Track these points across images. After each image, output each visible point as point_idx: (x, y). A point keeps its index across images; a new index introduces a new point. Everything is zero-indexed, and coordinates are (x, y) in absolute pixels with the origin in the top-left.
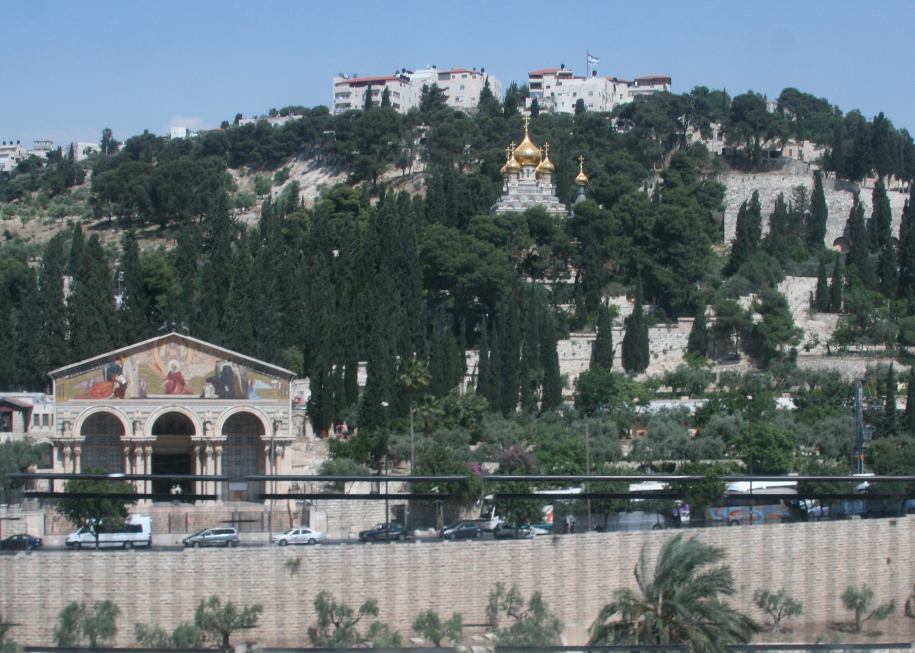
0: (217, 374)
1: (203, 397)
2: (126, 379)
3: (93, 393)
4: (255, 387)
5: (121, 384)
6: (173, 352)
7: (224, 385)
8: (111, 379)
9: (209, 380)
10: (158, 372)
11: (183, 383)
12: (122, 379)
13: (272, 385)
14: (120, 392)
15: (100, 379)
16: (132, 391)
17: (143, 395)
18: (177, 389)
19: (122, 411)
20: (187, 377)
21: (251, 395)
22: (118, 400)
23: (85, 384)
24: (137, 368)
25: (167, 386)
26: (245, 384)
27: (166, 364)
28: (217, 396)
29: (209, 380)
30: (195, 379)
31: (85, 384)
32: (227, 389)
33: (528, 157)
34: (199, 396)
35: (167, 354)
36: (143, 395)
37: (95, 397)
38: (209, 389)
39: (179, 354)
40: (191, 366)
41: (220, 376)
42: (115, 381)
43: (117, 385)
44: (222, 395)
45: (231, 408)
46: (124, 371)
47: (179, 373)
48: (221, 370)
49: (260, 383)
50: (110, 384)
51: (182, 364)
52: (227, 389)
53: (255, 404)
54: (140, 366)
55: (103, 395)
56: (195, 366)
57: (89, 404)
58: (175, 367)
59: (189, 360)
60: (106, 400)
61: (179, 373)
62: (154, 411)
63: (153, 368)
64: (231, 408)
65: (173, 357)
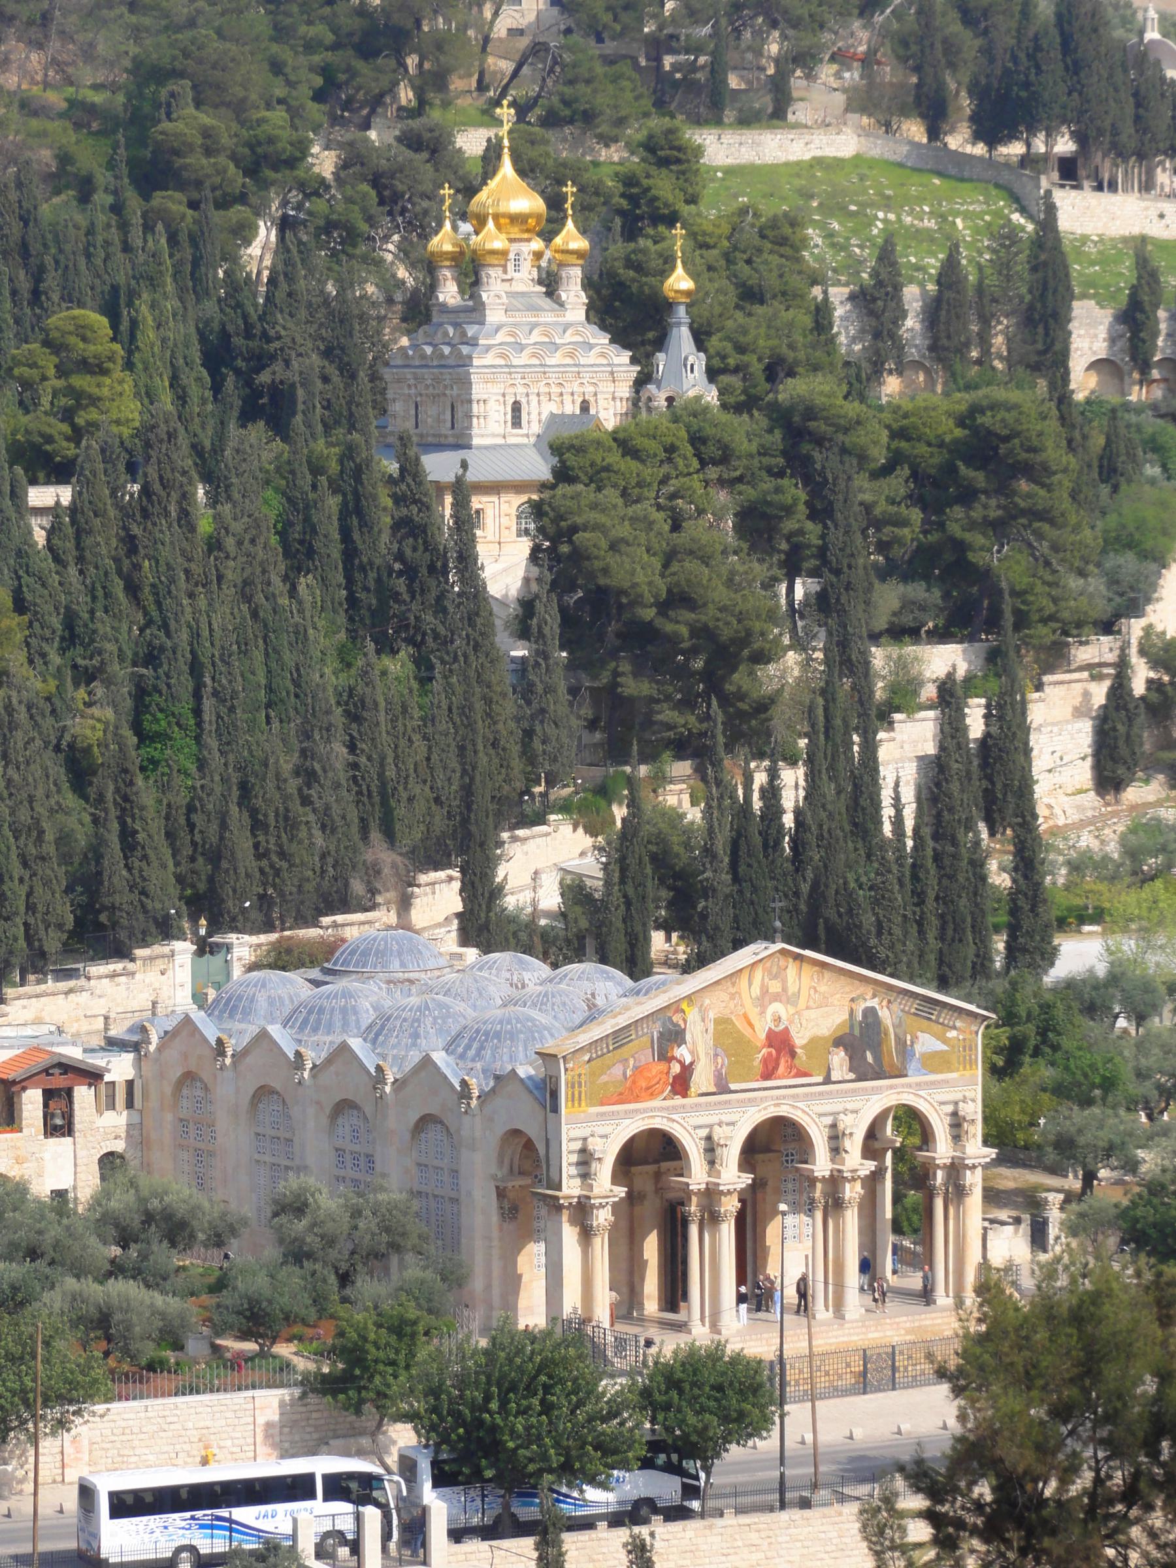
0: (852, 1027)
1: (827, 1081)
2: (692, 1053)
3: (630, 1093)
4: (919, 1049)
5: (682, 1063)
6: (775, 987)
7: (865, 1049)
8: (665, 1056)
9: (838, 1042)
10: (747, 1032)
11: (793, 1054)
12: (683, 1053)
13: (945, 1041)
14: (681, 1085)
15: (647, 1056)
16: (702, 1079)
17: (722, 1088)
18: (781, 1069)
19: (685, 1124)
20: (800, 1039)
21: (912, 1066)
22: (678, 1100)
23: (617, 1071)
24: (711, 1027)
25: (765, 1061)
26: (901, 1042)
27: (763, 1013)
28: (852, 1076)
29: (838, 1042)
30: (814, 1042)
31: (617, 1071)
32: (869, 1057)
33: (517, 219)
34: (820, 1079)
35: (765, 991)
36: (722, 1088)
37: (637, 1099)
38: (839, 1060)
39: (785, 989)
40: (806, 1013)
41: (857, 1032)
42: (673, 1058)
43: (676, 1068)
44: (862, 1072)
45: (879, 1098)
46: (688, 1037)
47: (786, 1030)
48: (860, 1017)
49: (926, 1043)
50: (662, 1066)
51: (792, 1010)
52: (869, 1057)
53: (918, 1084)
54: (718, 1022)
55: (651, 1092)
56: (813, 1014)
57: (628, 1114)
58: (778, 1020)
59: (802, 1003)
60: (656, 1103)
61: (786, 1030)
62: (738, 1123)
63: (740, 1024)
64: (879, 1098)
65: (776, 998)
